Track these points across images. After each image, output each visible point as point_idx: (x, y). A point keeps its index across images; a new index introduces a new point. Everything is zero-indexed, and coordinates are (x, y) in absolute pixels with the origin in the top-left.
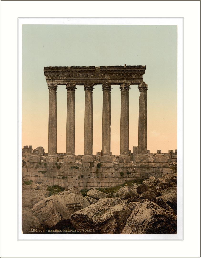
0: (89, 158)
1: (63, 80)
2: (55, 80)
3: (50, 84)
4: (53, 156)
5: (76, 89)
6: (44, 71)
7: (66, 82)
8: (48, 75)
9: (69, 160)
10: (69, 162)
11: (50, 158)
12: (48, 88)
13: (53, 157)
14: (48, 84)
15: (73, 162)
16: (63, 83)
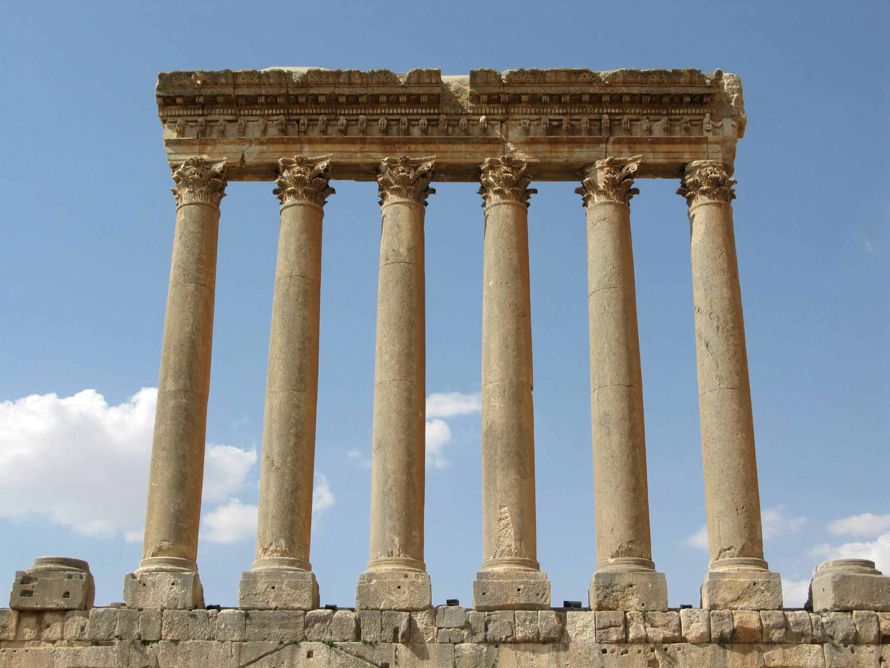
0: (403, 579)
1: (262, 143)
2: (214, 142)
3: (187, 164)
4: (170, 567)
5: (330, 198)
6: (158, 96)
7: (276, 156)
8: (179, 120)
9: (272, 596)
10: (273, 605)
11: (154, 584)
12: (174, 186)
13: (170, 578)
14: (175, 167)
15: (297, 605)
16: (260, 161)
